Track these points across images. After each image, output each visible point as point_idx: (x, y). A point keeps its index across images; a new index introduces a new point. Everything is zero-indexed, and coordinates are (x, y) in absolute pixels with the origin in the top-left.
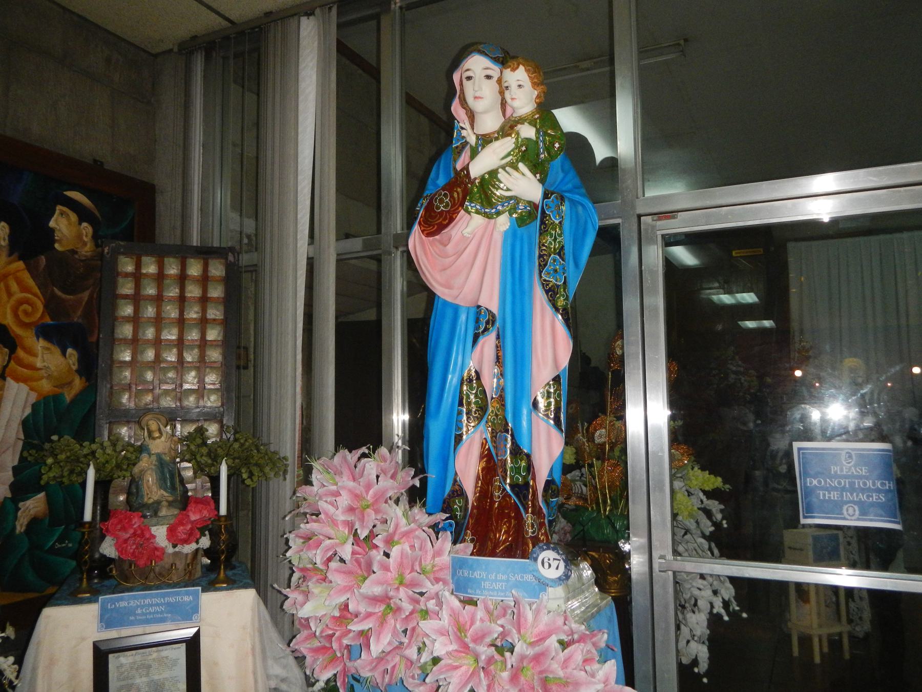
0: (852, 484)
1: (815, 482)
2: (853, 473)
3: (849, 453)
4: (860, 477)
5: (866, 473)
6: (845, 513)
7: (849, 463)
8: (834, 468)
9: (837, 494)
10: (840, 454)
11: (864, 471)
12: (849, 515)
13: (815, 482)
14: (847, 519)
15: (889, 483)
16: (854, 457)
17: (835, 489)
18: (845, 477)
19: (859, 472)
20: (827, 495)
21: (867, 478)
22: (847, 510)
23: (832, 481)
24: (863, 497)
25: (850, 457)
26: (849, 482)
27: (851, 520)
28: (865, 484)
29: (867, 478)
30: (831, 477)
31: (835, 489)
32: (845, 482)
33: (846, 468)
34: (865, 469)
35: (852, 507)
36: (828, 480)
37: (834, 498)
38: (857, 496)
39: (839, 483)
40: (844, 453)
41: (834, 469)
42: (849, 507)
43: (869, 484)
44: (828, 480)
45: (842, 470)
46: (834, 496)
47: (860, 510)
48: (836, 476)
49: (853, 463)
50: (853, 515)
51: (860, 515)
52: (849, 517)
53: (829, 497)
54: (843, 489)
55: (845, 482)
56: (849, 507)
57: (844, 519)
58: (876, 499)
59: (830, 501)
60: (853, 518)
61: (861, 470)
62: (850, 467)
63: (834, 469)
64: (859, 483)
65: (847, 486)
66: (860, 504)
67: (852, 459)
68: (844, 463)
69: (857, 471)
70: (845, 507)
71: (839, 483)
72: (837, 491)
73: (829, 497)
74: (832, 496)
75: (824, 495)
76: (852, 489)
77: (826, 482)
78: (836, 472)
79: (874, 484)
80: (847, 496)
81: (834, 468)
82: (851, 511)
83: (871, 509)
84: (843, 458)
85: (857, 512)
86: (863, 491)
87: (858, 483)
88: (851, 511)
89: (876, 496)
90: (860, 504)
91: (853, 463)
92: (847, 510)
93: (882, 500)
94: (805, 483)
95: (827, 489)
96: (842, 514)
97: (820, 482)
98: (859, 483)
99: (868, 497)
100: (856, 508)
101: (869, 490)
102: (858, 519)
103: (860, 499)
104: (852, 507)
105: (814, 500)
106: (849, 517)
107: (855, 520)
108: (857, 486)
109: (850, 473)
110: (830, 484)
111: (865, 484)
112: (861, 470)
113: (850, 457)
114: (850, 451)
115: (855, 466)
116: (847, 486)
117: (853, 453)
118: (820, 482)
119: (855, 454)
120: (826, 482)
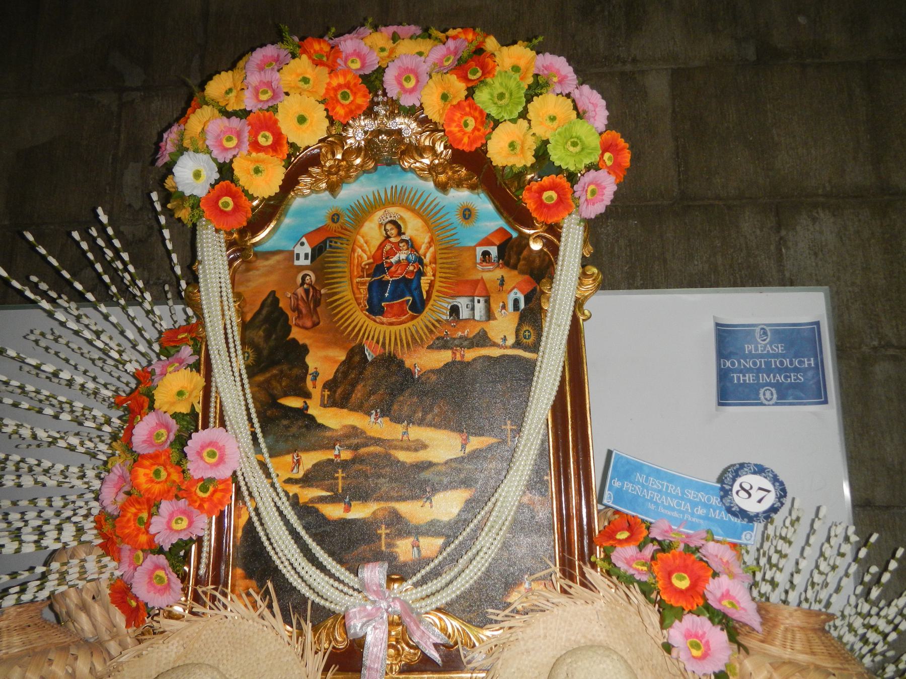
1: (728, 364)
2: (768, 351)
5: (782, 350)
6: (761, 396)
7: (764, 340)
8: (748, 347)
9: (753, 376)
11: (780, 349)
12: (766, 399)
13: (728, 364)
15: (809, 360)
16: (769, 333)
17: (750, 370)
18: (761, 356)
19: (775, 351)
20: (741, 378)
21: (783, 356)
22: (764, 394)
23: (747, 362)
24: (781, 378)
25: (765, 333)
26: (765, 361)
27: (769, 405)
28: (782, 363)
29: (783, 356)
30: (745, 357)
31: (750, 370)
32: (761, 362)
33: (761, 347)
34: (782, 346)
35: (769, 390)
37: (749, 380)
38: (774, 377)
39: (755, 364)
40: (758, 329)
41: (748, 348)
42: (766, 390)
43: (787, 362)
45: (757, 349)
46: (749, 378)
47: (778, 393)
48: (751, 356)
49: (768, 340)
50: (771, 399)
51: (778, 399)
52: (766, 402)
53: (744, 381)
54: (759, 370)
55: (761, 362)
56: (766, 390)
57: (762, 404)
58: (795, 380)
59: (744, 384)
60: (771, 403)
61: (778, 348)
62: (765, 346)
63: (748, 348)
64: (775, 362)
65: (763, 366)
66: (778, 386)
67: (767, 336)
68: (759, 340)
69: (773, 349)
70: (762, 391)
71: (755, 364)
72: (752, 373)
73: (744, 381)
74: (747, 378)
75: (739, 378)
76: (769, 370)
77: (739, 363)
78: (750, 351)
79: (791, 363)
80: (764, 378)
81: (748, 347)
82: (768, 393)
83: (790, 392)
84: (757, 335)
85: (775, 396)
86: (780, 371)
87: (775, 363)
88: (768, 395)
89: (794, 376)
90: (778, 386)
91: (768, 340)
92: (764, 394)
93: (800, 380)
95: (741, 371)
96: (759, 399)
97: (733, 364)
98: (775, 362)
99: (786, 377)
100: (774, 391)
101: (787, 370)
102: (776, 404)
103: (778, 380)
104: (769, 390)
105: (728, 384)
106: (766, 402)
107: (773, 405)
108: (773, 366)
109: (765, 352)
110: (744, 366)
111: (782, 363)
112: (778, 348)
114: (765, 327)
115: (771, 343)
116: (763, 366)
117: (767, 329)
118: (733, 364)
120: (739, 363)
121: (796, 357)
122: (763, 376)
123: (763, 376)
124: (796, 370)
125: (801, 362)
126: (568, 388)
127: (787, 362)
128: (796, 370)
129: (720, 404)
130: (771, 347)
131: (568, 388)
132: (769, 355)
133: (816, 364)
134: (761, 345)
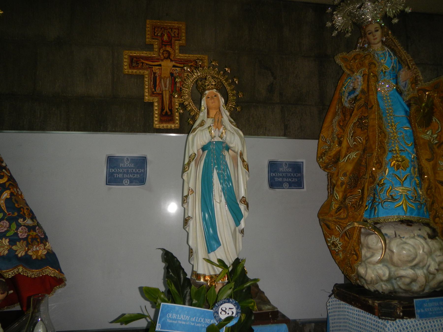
0: (128, 171)
1: (113, 170)
2: (128, 166)
3: (128, 158)
6: (124, 182)
7: (127, 162)
10: (124, 159)
11: (132, 166)
12: (125, 183)
14: (125, 185)
15: (142, 170)
16: (129, 160)
17: (121, 173)
18: (126, 168)
22: (125, 182)
25: (128, 160)
27: (126, 185)
31: (121, 173)
32: (125, 170)
36: (118, 169)
38: (129, 176)
44: (118, 169)
46: (120, 176)
47: (130, 181)
48: (122, 168)
50: (127, 183)
51: (130, 183)
52: (125, 184)
53: (118, 176)
54: (124, 173)
55: (125, 170)
57: (124, 185)
61: (132, 165)
62: (127, 164)
64: (130, 170)
67: (129, 161)
68: (126, 163)
69: (130, 166)
70: (124, 180)
73: (118, 176)
75: (116, 176)
76: (127, 173)
79: (136, 171)
80: (125, 176)
82: (126, 182)
84: (125, 160)
85: (129, 182)
88: (126, 182)
92: (125, 182)
93: (138, 177)
94: (109, 171)
98: (130, 170)
99: (133, 176)
100: (128, 180)
106: (125, 184)
107: (128, 185)
109: (127, 166)
110: (119, 171)
111: (132, 171)
112: (132, 165)
113: (128, 160)
114: (128, 157)
115: (129, 163)
117: (129, 158)
119: (130, 159)
122: (125, 175)
123: (125, 175)
124: (137, 173)
125: (139, 171)
127: (134, 170)
128: (137, 173)
129: (107, 184)
130: (129, 165)
132: (128, 168)
133: (144, 171)
134: (126, 164)
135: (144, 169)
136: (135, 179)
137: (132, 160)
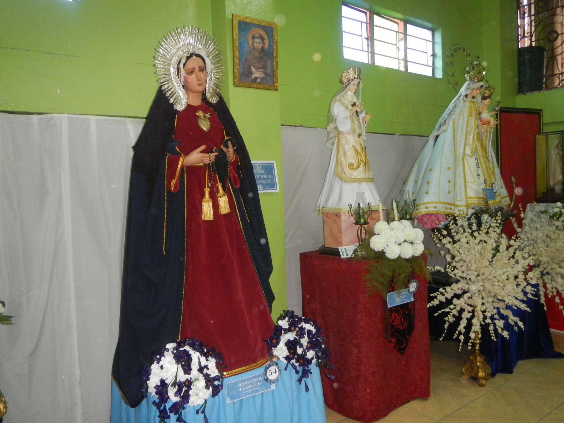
0: (260, 177)
4: (262, 174)
11: (263, 172)
25: (259, 166)
40: (257, 165)
51: (263, 188)
60: (261, 190)
82: (260, 187)
83: (267, 186)
84: (257, 167)
85: (262, 188)
86: (263, 179)
87: (262, 176)
88: (260, 187)
100: (262, 186)
101: (265, 179)
102: (263, 190)
113: (259, 166)
115: (261, 170)
117: (260, 165)
121: (268, 174)
124: (268, 179)
125: (269, 176)
126: (230, 186)
128: (268, 179)
131: (230, 186)
135: (273, 174)
136: (267, 184)
137: (262, 166)
